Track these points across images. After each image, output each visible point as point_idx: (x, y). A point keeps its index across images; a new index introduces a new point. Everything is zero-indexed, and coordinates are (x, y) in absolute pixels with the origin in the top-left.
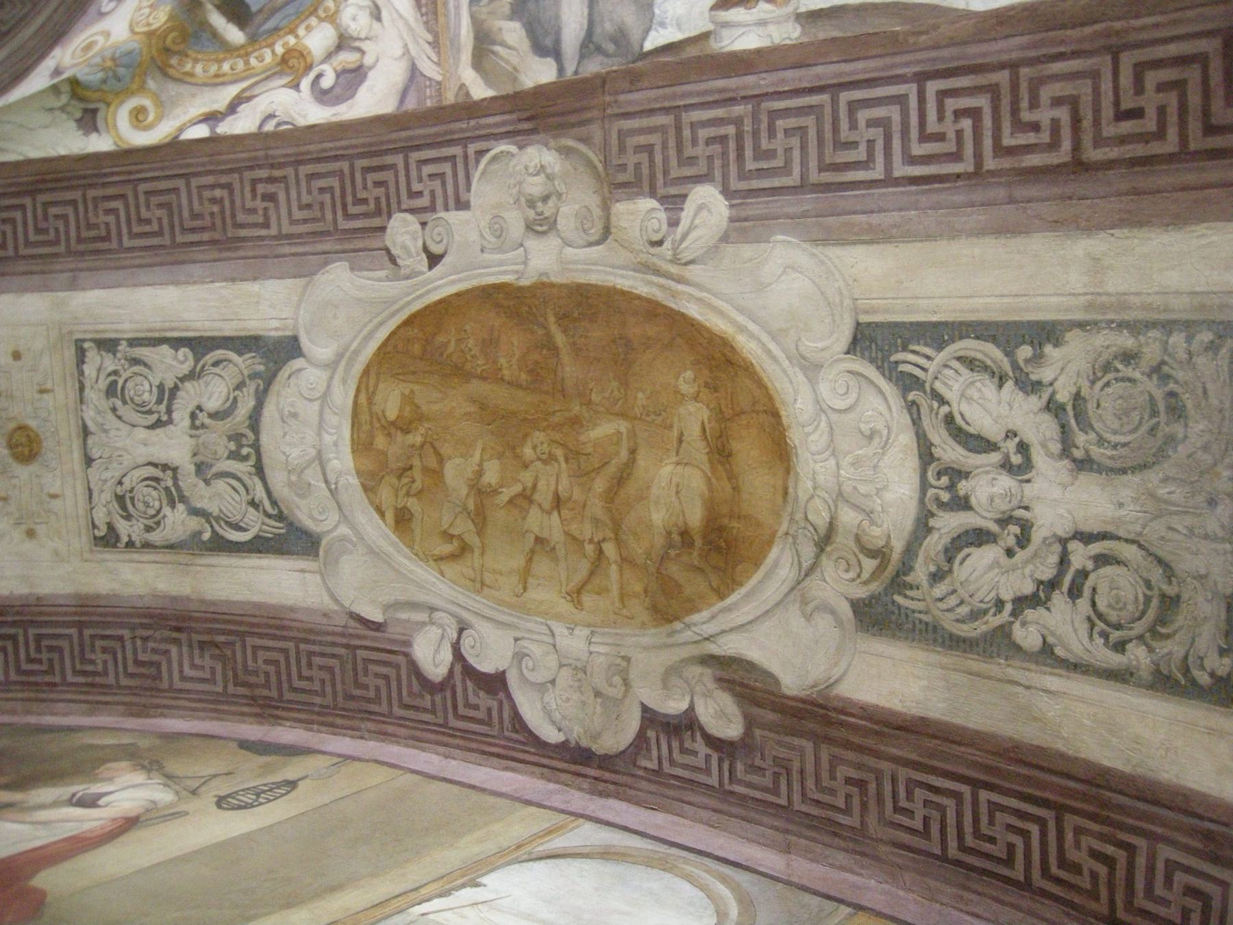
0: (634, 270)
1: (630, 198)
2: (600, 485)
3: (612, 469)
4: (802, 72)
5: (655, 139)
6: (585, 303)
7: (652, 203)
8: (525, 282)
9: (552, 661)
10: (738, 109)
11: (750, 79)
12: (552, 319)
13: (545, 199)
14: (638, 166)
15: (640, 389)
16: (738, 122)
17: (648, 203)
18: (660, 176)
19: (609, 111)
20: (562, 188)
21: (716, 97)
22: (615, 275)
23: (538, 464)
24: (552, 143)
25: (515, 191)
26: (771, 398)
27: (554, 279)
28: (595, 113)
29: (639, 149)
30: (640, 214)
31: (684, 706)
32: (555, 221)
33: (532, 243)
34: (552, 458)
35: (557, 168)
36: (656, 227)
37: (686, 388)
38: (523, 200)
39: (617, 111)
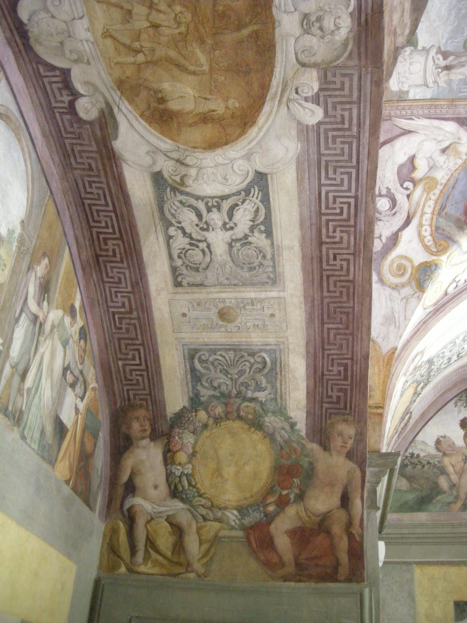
0: (284, 78)
1: (319, 79)
2: (172, 53)
3: (183, 61)
4: (366, 155)
5: (347, 91)
6: (265, 47)
7: (316, 89)
8: (274, 10)
9: (65, 17)
10: (355, 129)
11: (367, 134)
12: (255, 28)
13: (321, 29)
14: (334, 83)
15: (226, 78)
16: (349, 129)
17: (316, 87)
18: (329, 93)
19: (363, 69)
20: (326, 40)
21: (362, 120)
22: (281, 68)
23: (173, 15)
24: (351, 35)
25: (327, 8)
26: (233, 141)
27: (277, 31)
28: (363, 62)
29: (343, 83)
30: (311, 82)
31: (82, 92)
32: (309, 34)
33: (296, 17)
34: (179, 24)
35: (337, 38)
36: (304, 91)
37: (231, 102)
38: (321, 13)
39: (363, 73)
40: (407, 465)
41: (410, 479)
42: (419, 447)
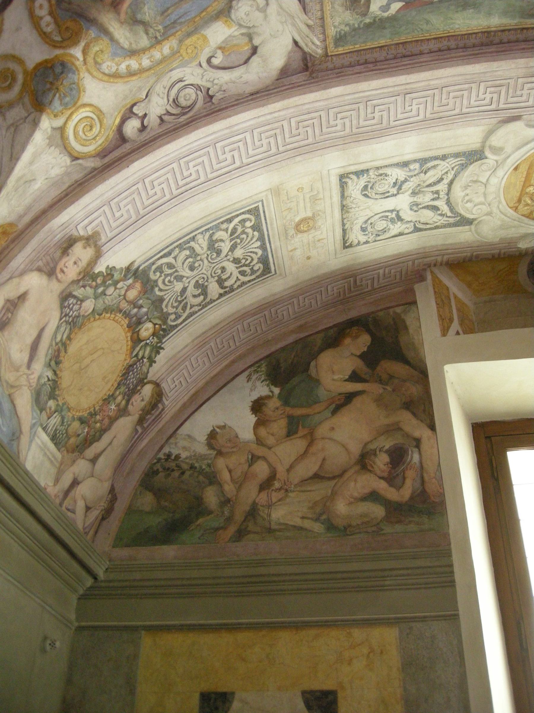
40: (157, 472)
41: (159, 493)
42: (182, 443)
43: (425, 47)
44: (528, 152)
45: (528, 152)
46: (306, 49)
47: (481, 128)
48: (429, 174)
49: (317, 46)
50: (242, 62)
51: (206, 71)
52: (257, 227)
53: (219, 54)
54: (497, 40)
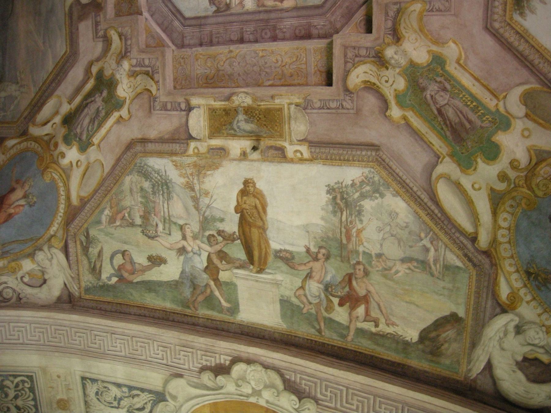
43: (133, 310)
44: (193, 406)
45: (193, 406)
46: (71, 290)
47: (161, 376)
48: (136, 399)
49: (76, 290)
50: (38, 285)
51: (19, 283)
52: (32, 390)
53: (27, 276)
54: (171, 319)
